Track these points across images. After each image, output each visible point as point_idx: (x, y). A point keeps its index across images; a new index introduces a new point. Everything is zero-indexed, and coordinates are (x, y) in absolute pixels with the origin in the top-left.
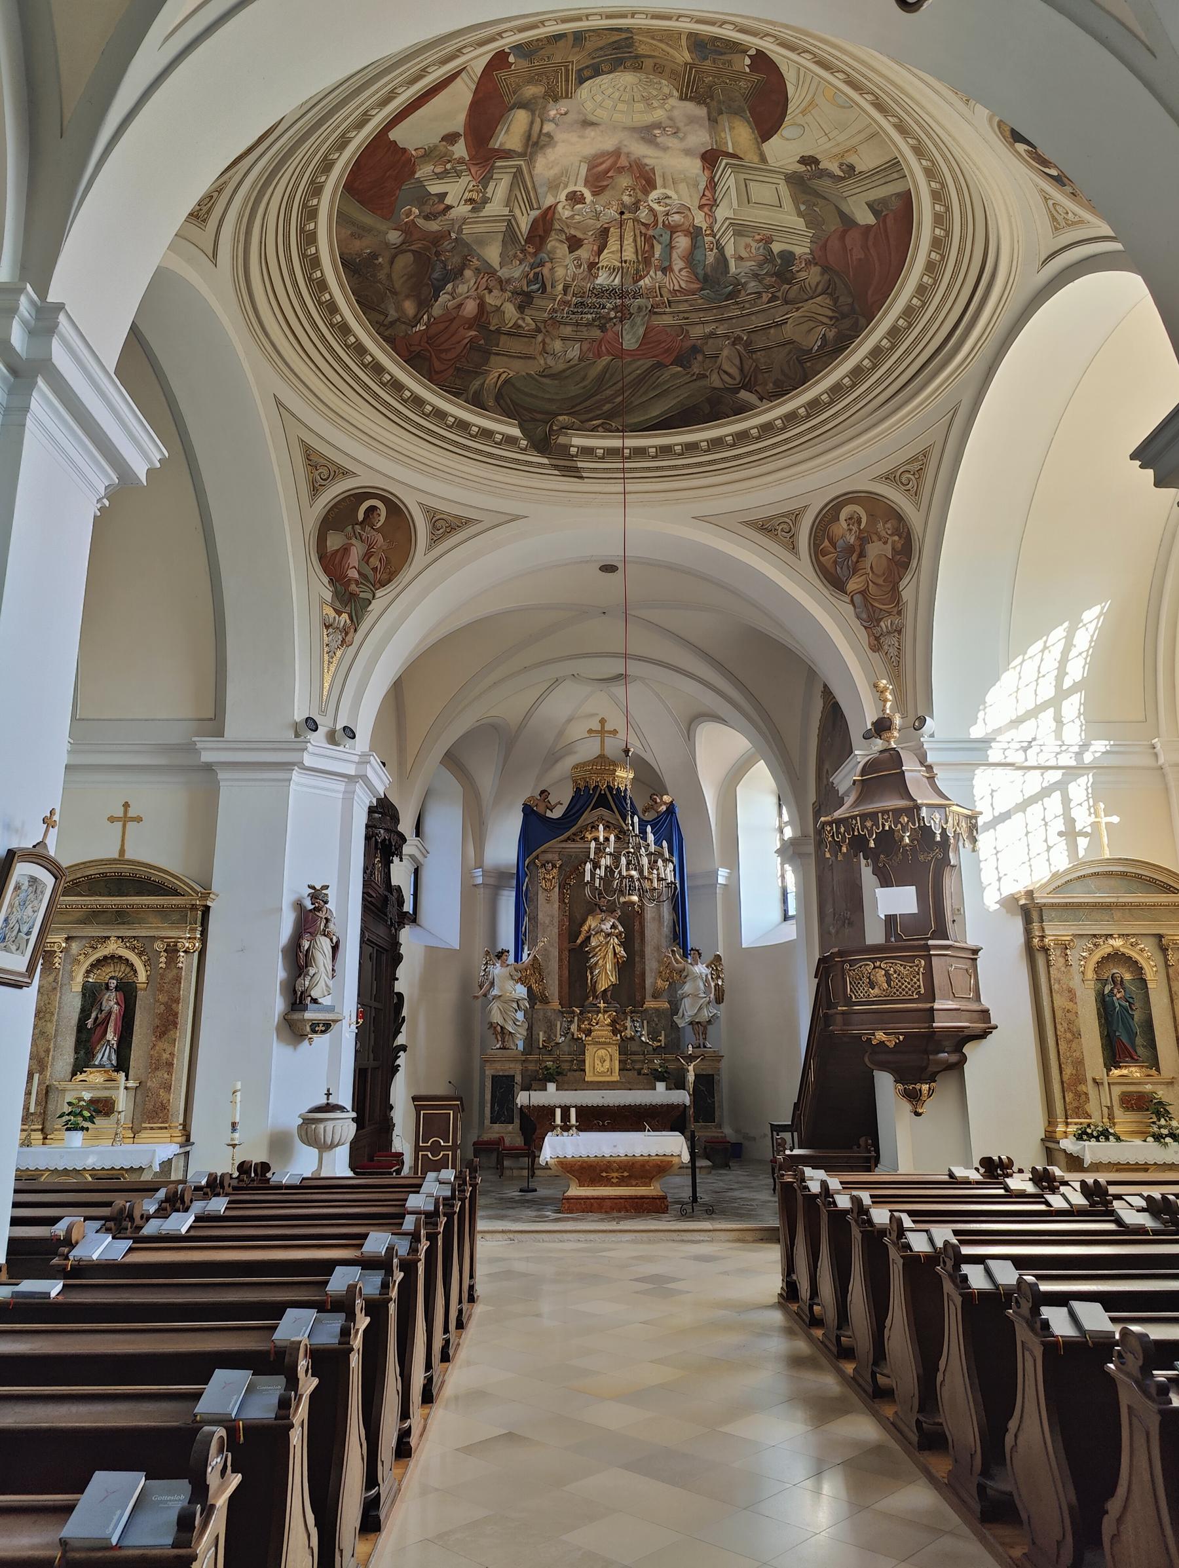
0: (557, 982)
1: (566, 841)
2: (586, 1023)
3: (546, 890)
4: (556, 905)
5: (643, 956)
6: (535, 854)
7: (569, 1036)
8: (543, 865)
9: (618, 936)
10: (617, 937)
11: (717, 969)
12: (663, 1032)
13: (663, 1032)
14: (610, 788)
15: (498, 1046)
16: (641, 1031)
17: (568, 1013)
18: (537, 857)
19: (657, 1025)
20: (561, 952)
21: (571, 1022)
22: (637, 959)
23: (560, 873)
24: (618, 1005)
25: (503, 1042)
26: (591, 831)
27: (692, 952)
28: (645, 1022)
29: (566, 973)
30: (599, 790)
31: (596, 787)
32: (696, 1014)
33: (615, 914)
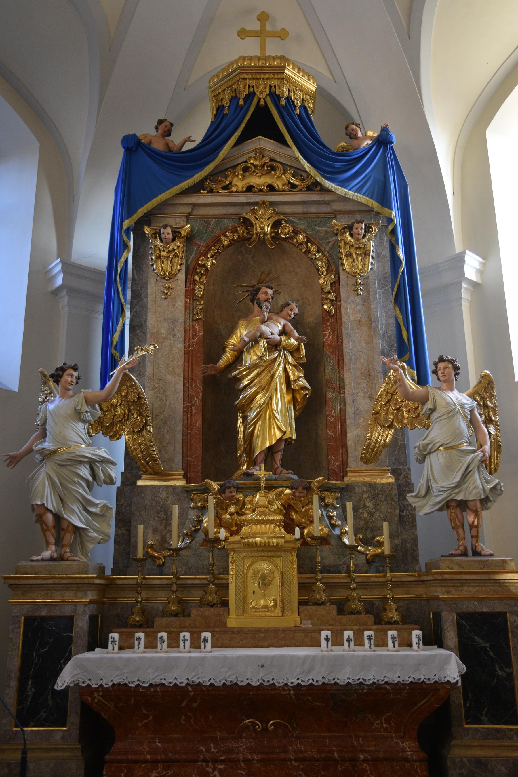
0: (179, 437)
1: (196, 189)
2: (232, 509)
3: (163, 277)
4: (181, 302)
5: (341, 389)
6: (141, 212)
7: (200, 536)
8: (157, 234)
9: (294, 351)
10: (291, 353)
11: (486, 406)
12: (385, 525)
13: (385, 525)
14: (275, 97)
15: (47, 554)
16: (341, 527)
17: (198, 491)
18: (146, 220)
19: (371, 514)
20: (188, 381)
21: (204, 509)
22: (330, 394)
23: (188, 252)
24: (295, 477)
25: (59, 542)
26: (244, 176)
27: (441, 365)
28: (349, 506)
29: (198, 421)
30: (255, 101)
31: (250, 96)
32: (459, 485)
33: (287, 311)
